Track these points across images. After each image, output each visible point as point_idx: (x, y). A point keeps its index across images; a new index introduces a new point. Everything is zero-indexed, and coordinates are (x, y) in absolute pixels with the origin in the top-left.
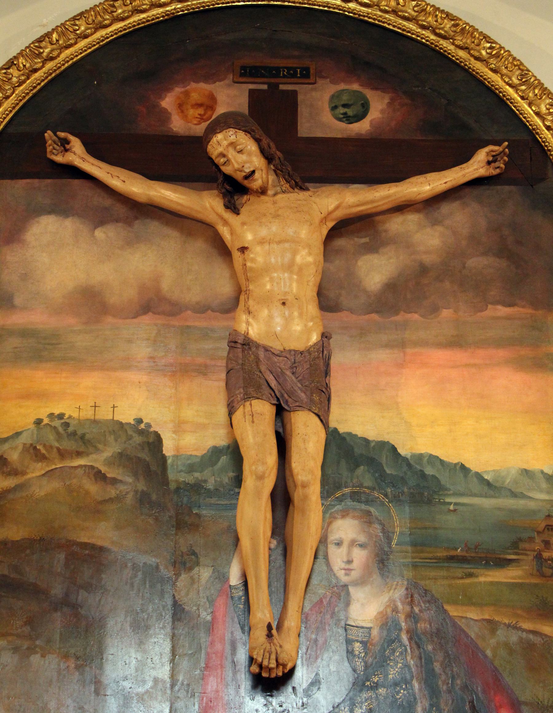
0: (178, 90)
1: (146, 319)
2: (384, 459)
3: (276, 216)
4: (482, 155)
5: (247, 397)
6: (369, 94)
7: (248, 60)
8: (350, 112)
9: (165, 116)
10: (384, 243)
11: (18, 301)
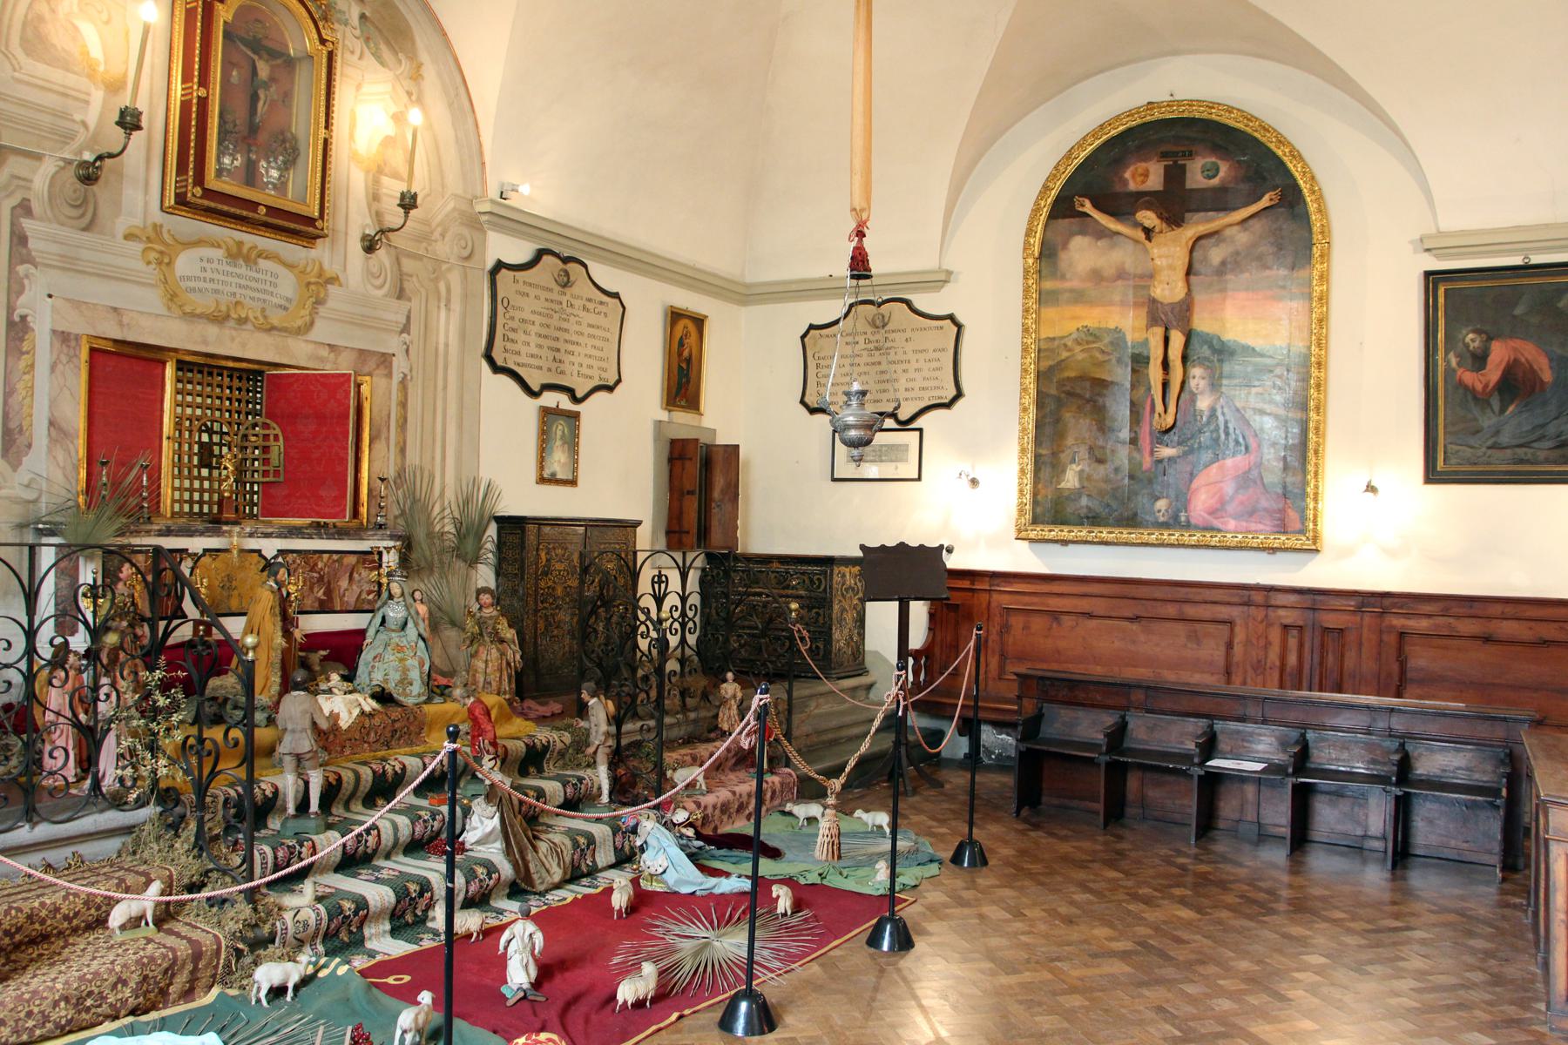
0: (1132, 168)
1: (1119, 283)
2: (1215, 342)
3: (1165, 245)
4: (1267, 197)
5: (1152, 326)
6: (1219, 162)
7: (1164, 148)
8: (1210, 173)
9: (1125, 183)
10: (1224, 241)
11: (1068, 276)
